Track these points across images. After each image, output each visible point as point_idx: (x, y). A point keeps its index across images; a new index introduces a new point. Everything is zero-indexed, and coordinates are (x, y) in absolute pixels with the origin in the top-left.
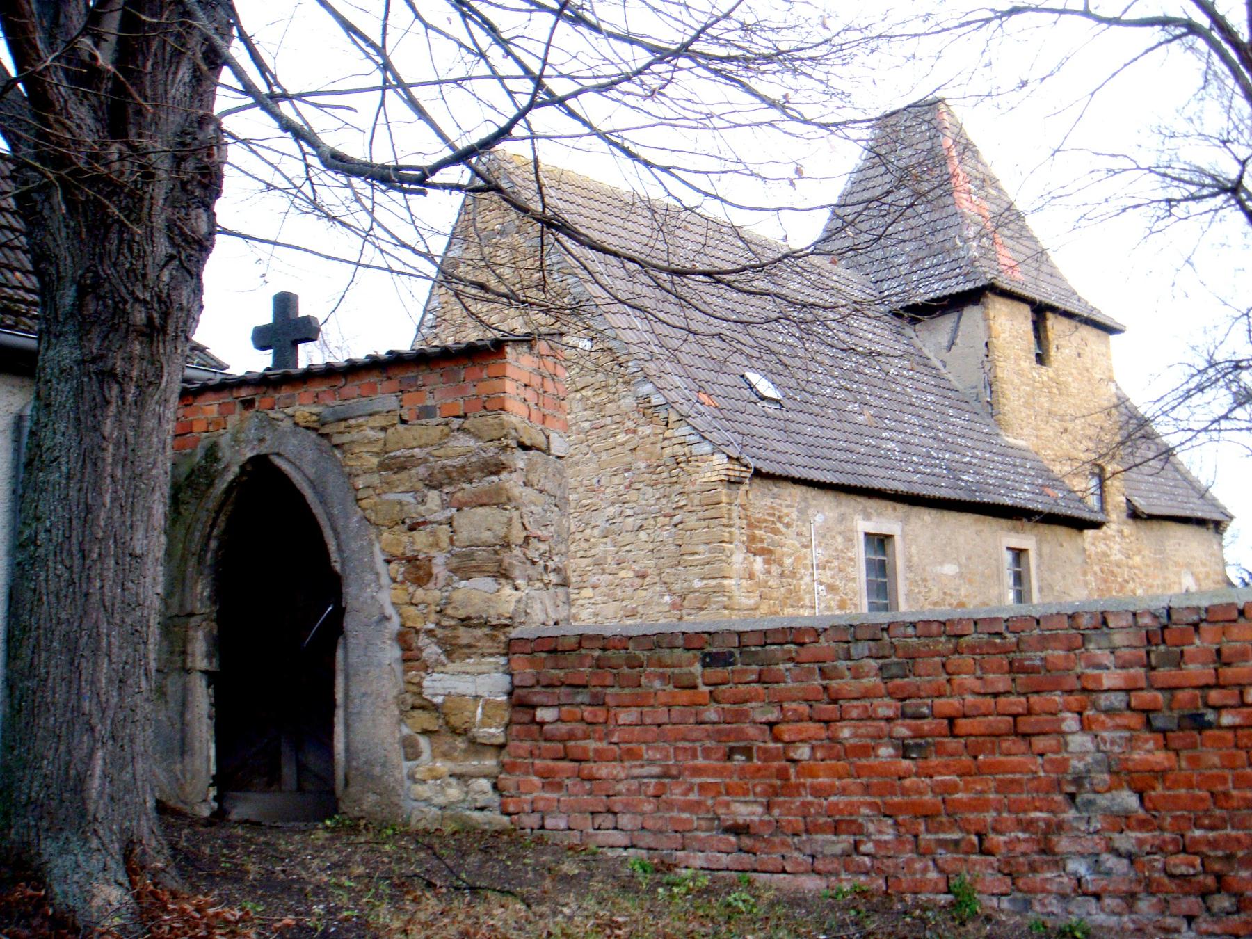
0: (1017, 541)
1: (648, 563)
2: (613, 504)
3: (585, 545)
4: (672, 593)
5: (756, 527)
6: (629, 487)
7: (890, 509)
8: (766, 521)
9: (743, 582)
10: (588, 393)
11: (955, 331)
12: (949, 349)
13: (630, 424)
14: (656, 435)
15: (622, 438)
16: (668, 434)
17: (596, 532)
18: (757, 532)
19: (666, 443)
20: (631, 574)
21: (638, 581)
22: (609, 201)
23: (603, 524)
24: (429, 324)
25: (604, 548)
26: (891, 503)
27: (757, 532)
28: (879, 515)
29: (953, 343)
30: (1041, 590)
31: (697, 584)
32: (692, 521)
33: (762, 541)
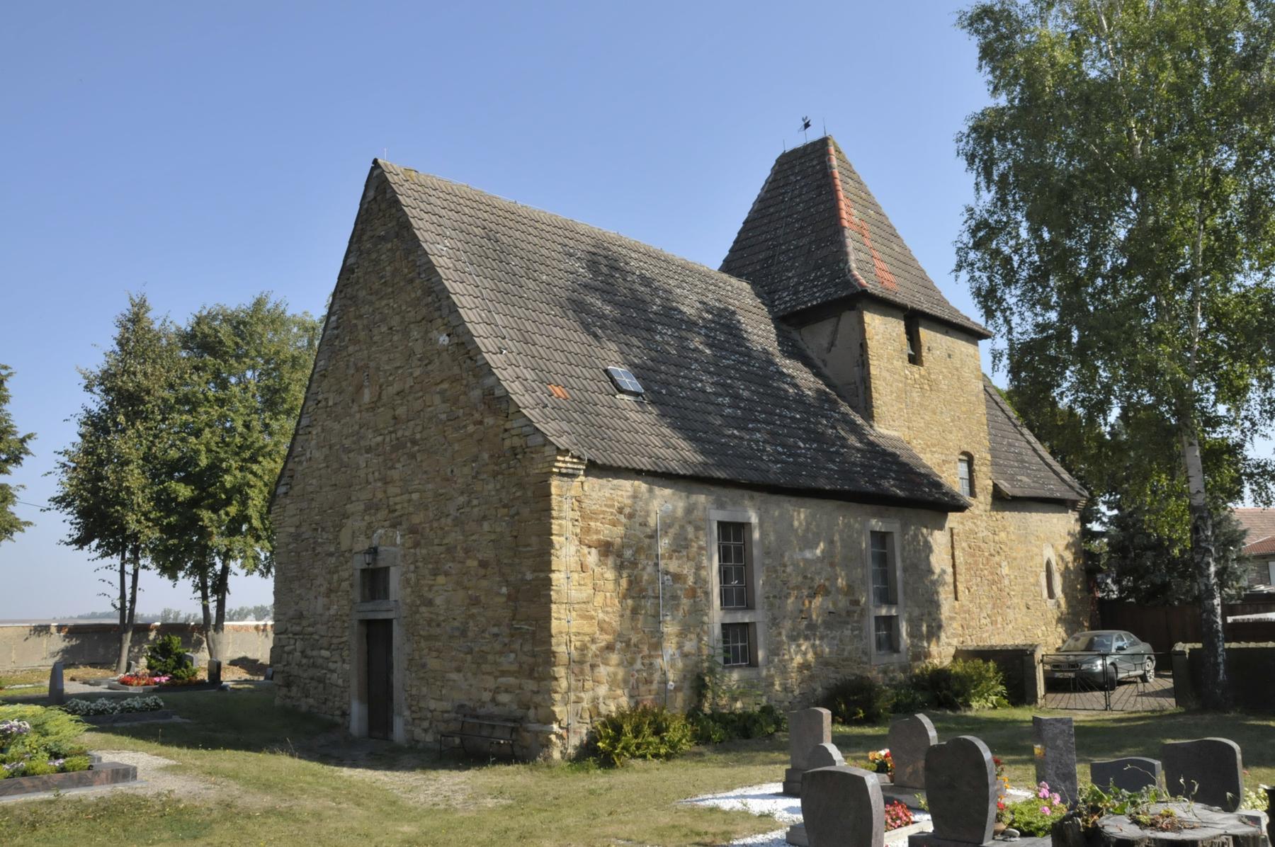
0: (876, 524)
1: (488, 554)
2: (462, 493)
3: (440, 532)
4: (508, 583)
5: (591, 519)
6: (474, 478)
7: (746, 496)
8: (604, 512)
9: (575, 576)
10: (445, 386)
11: (835, 332)
12: (829, 350)
13: (477, 416)
14: (498, 426)
15: (471, 428)
16: (508, 426)
17: (449, 521)
18: (592, 524)
19: (506, 435)
20: (475, 563)
21: (482, 572)
22: (549, 229)
23: (453, 512)
24: (334, 325)
25: (455, 537)
26: (750, 492)
27: (592, 524)
28: (734, 504)
29: (832, 344)
30: (905, 570)
31: (529, 576)
32: (526, 512)
33: (598, 532)
